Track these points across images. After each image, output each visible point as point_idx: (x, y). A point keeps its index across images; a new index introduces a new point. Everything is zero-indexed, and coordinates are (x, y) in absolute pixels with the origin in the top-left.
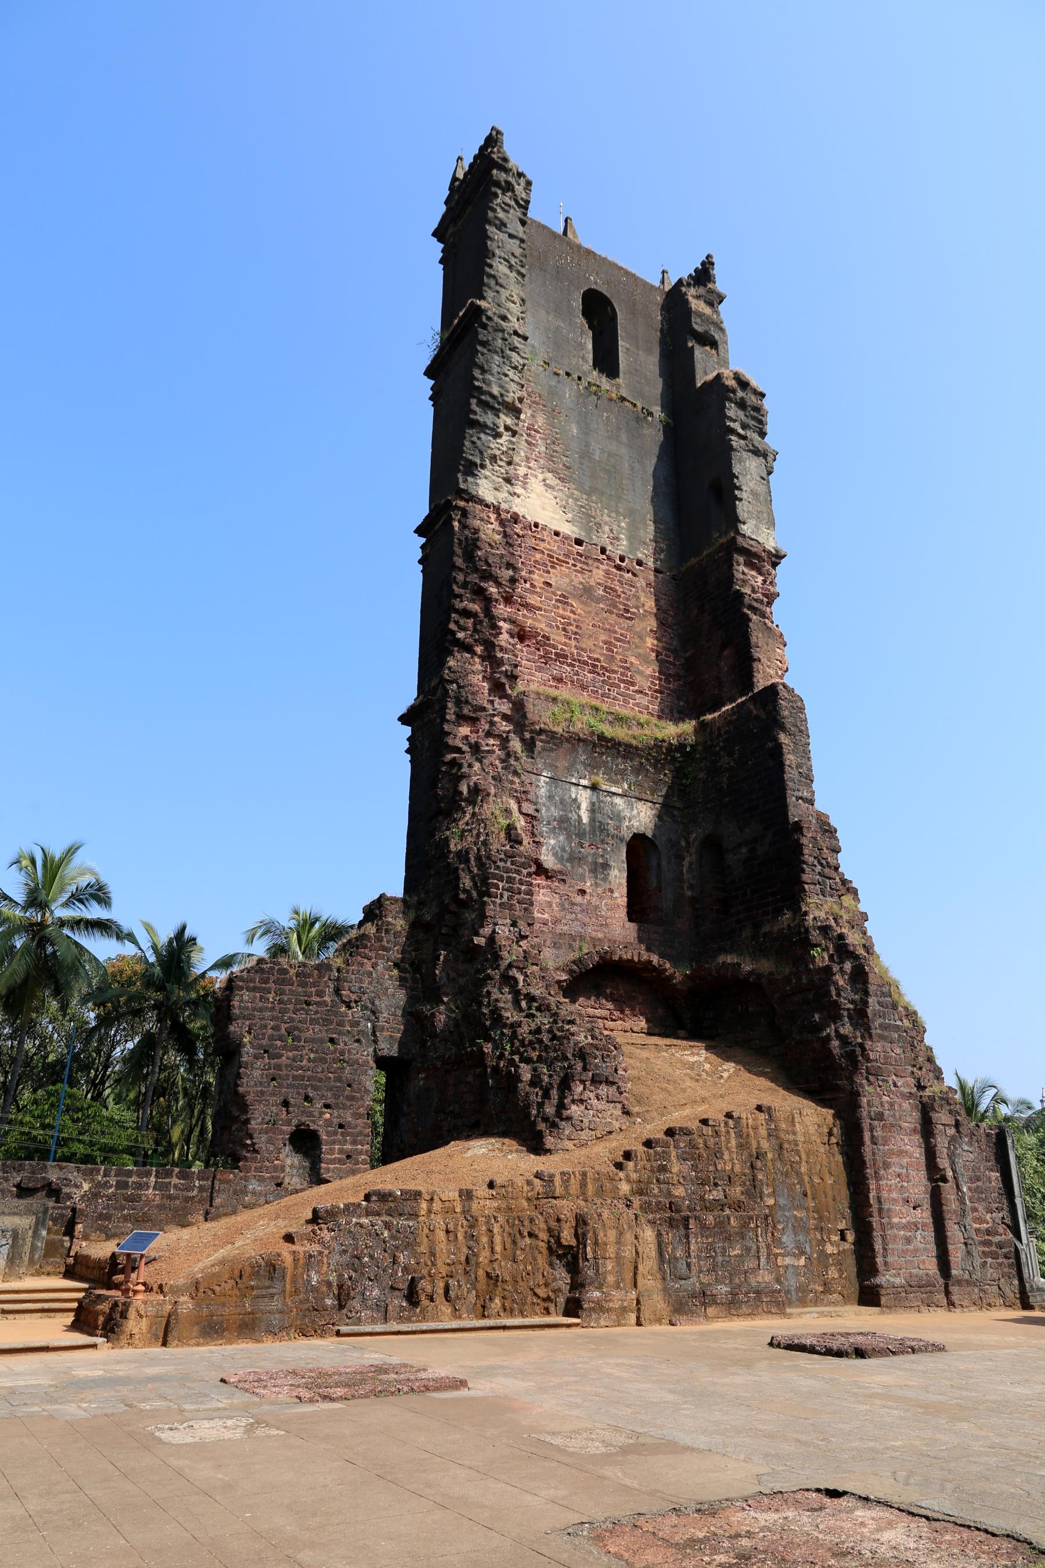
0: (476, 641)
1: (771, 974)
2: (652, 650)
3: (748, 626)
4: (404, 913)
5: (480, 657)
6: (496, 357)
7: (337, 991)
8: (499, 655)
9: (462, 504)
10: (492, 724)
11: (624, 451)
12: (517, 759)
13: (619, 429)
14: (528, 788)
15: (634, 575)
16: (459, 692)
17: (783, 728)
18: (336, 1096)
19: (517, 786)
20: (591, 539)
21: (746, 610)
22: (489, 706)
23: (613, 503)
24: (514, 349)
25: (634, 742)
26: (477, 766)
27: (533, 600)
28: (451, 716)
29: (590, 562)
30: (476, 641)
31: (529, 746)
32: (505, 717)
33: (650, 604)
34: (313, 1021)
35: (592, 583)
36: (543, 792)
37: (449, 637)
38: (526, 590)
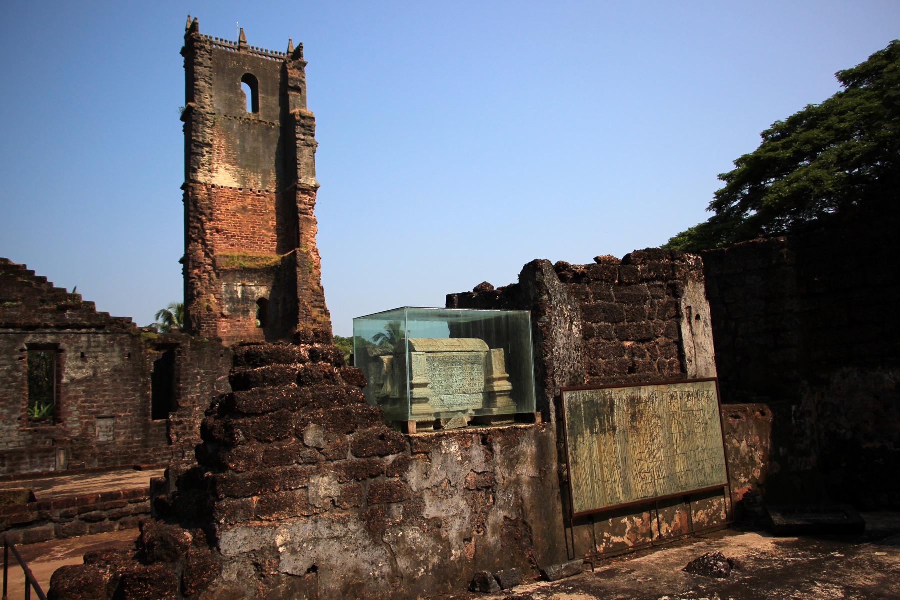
2: (272, 226)
3: (299, 221)
6: (201, 125)
9: (192, 185)
10: (205, 268)
11: (261, 145)
13: (258, 135)
14: (218, 290)
15: (265, 197)
17: (299, 266)
19: (214, 290)
23: (256, 169)
24: (208, 120)
25: (258, 268)
26: (199, 284)
27: (221, 217)
28: (191, 267)
29: (245, 196)
31: (218, 275)
32: (210, 265)
33: (272, 208)
35: (246, 205)
36: (224, 290)
38: (219, 214)
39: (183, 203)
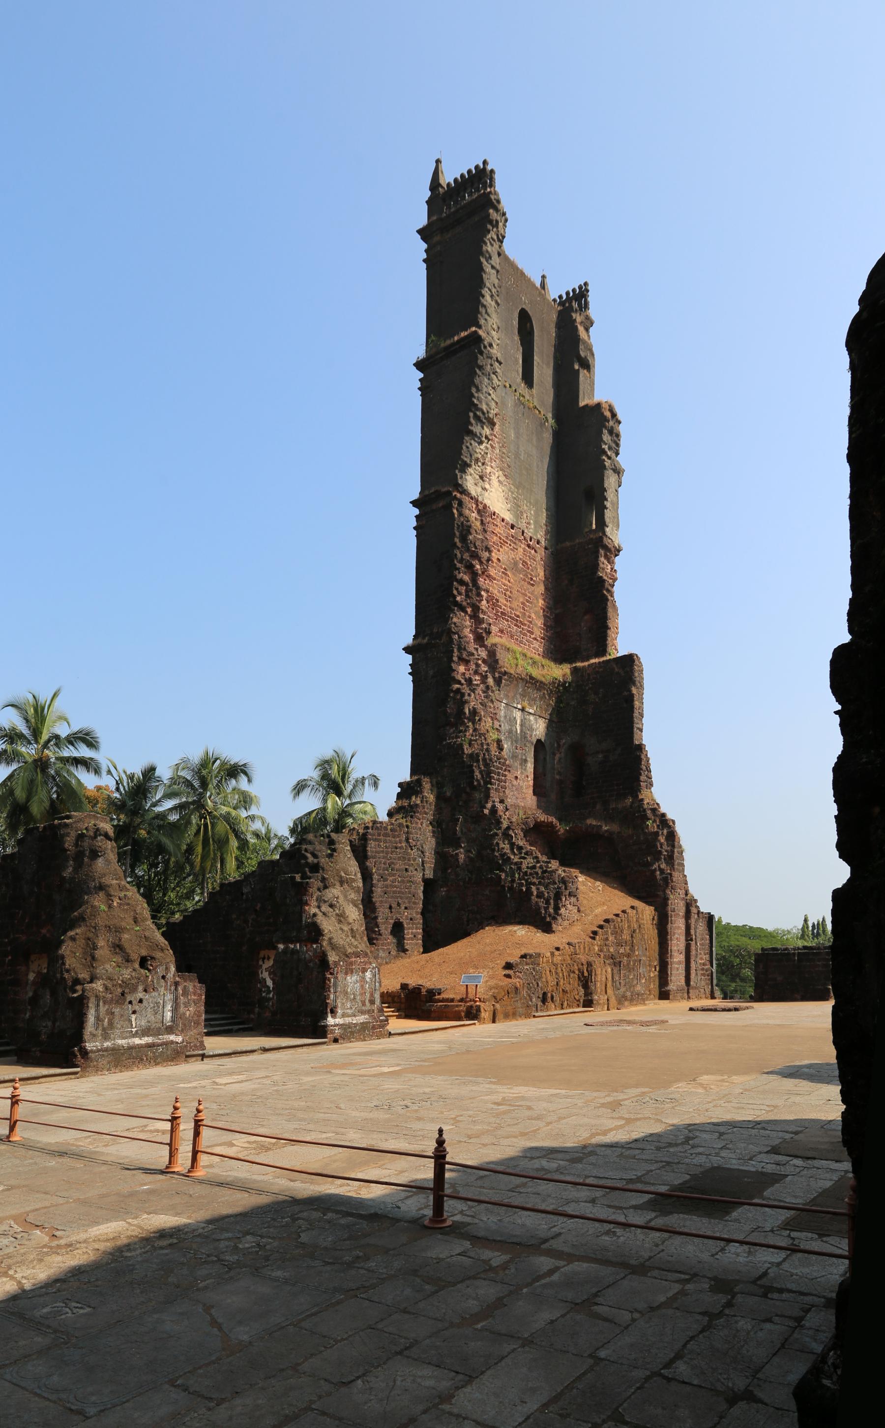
0: (468, 604)
1: (619, 833)
2: (541, 608)
4: (431, 790)
5: (469, 616)
7: (407, 840)
8: (481, 616)
10: (478, 665)
12: (493, 691)
15: (536, 551)
16: (460, 642)
18: (409, 902)
20: (518, 525)
21: (605, 592)
22: (475, 652)
28: (455, 659)
30: (468, 604)
32: (484, 661)
34: (399, 859)
36: (502, 713)
37: (451, 599)
39: (415, 532)
